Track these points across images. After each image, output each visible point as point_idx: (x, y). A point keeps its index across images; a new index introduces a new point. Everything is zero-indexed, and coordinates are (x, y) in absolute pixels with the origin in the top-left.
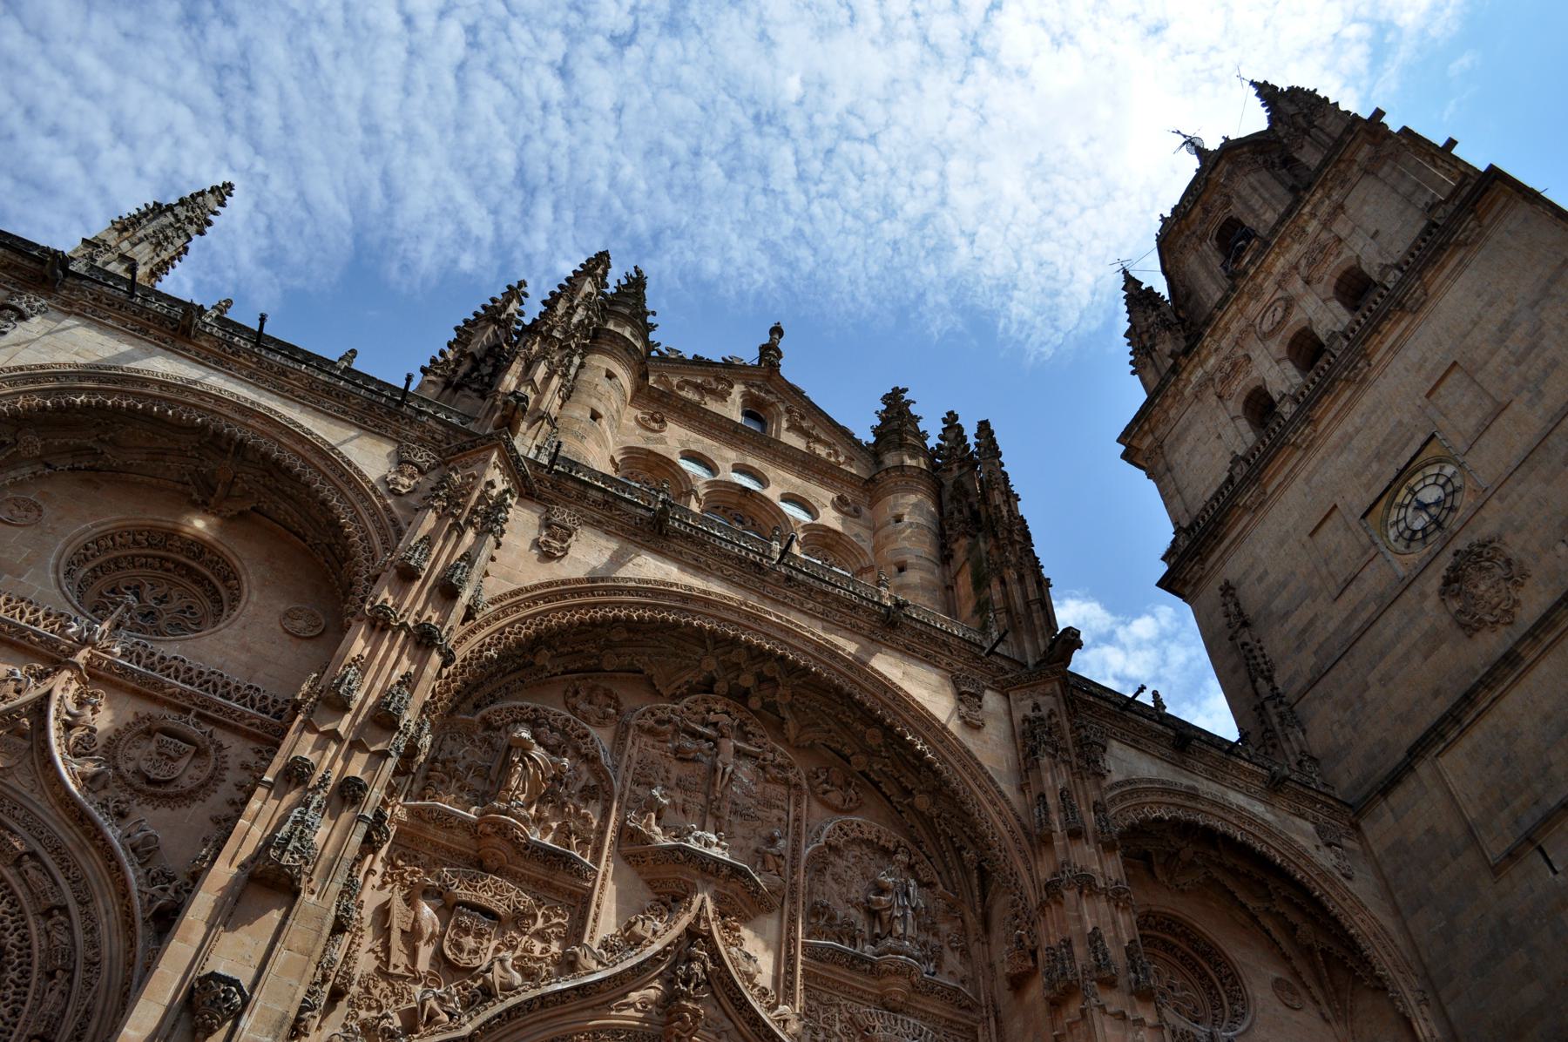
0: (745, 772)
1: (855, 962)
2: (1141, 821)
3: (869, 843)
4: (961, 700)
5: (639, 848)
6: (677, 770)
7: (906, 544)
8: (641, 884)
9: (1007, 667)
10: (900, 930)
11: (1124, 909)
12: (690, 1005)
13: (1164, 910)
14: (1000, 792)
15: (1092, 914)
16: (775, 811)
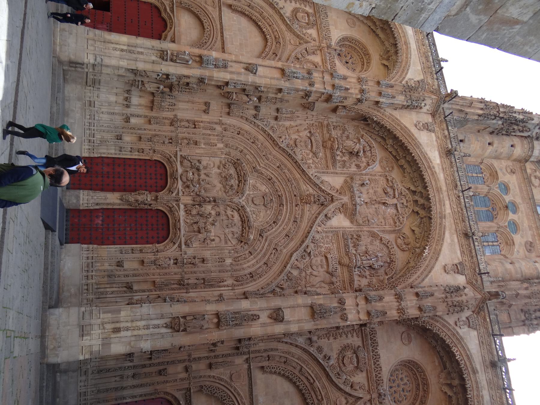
0: (391, 211)
1: (346, 246)
2: (448, 346)
3: (390, 251)
4: (453, 265)
5: (350, 181)
6: (380, 190)
7: (524, 264)
8: (340, 185)
9: (478, 283)
10: (363, 258)
11: (399, 313)
12: (312, 198)
13: (428, 378)
14: (423, 280)
15: (389, 299)
16: (383, 221)
